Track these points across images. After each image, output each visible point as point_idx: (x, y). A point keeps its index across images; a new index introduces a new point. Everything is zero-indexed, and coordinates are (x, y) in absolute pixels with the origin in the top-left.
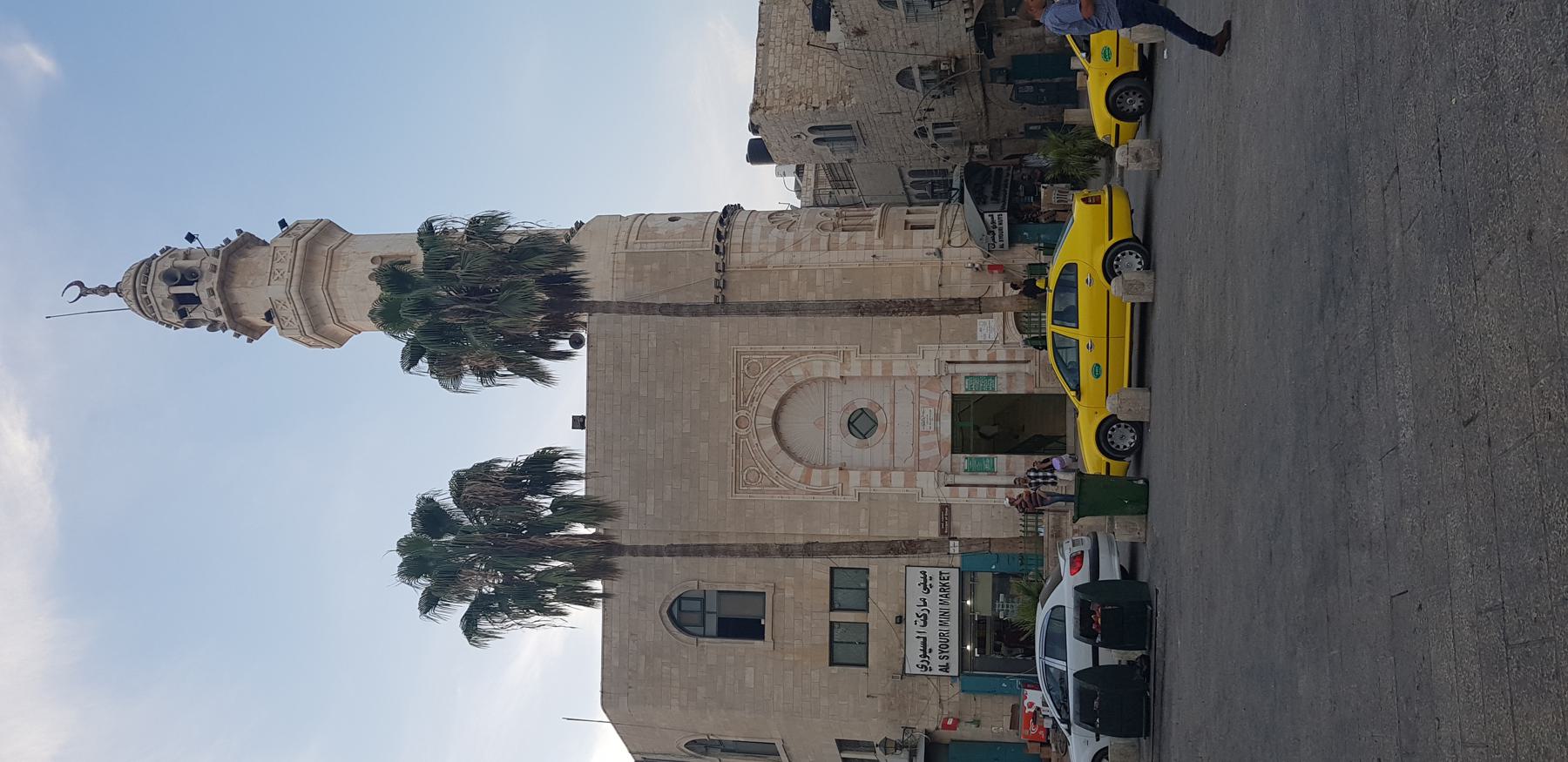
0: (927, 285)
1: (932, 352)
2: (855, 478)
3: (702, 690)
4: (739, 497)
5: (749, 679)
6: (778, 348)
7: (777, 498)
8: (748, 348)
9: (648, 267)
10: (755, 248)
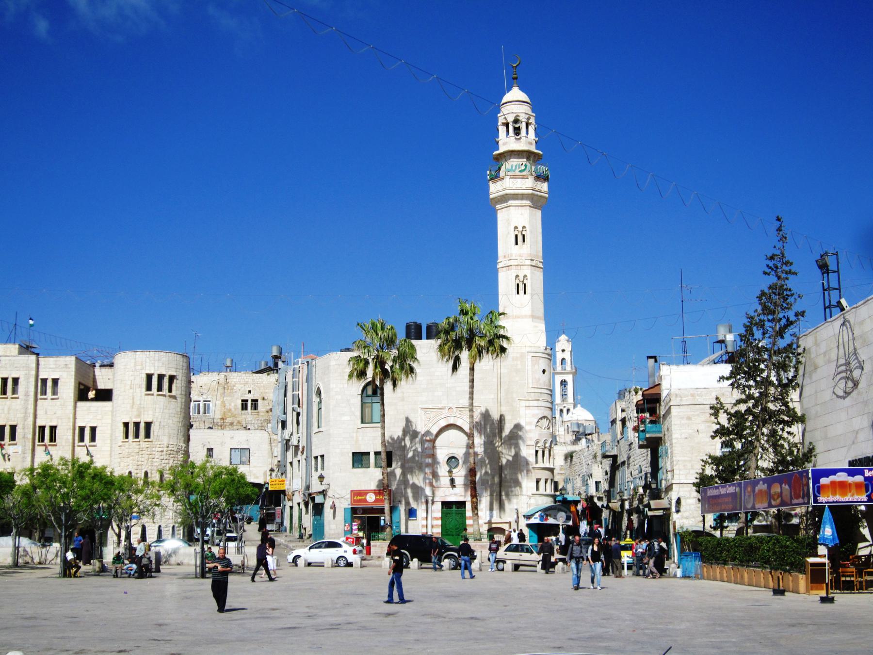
3: (340, 397)
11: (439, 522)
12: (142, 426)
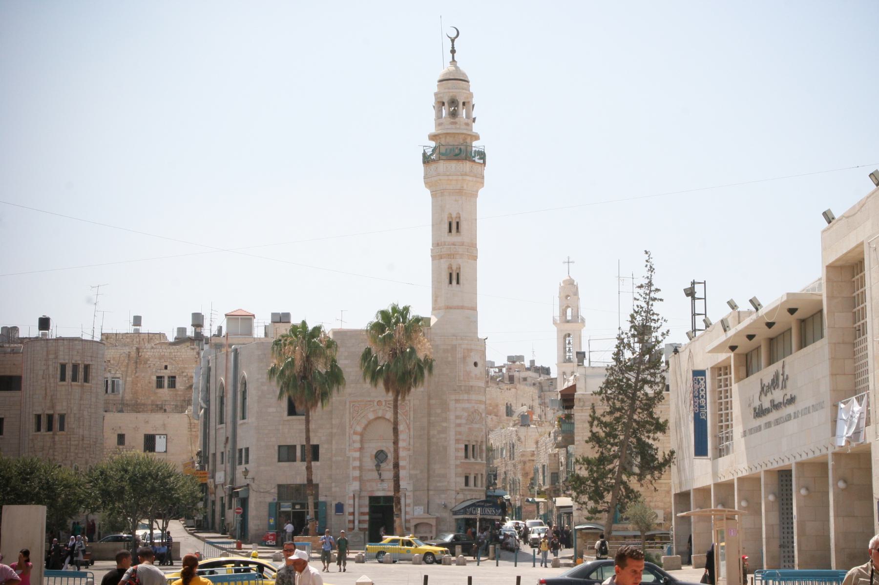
0: (439, 484)
1: (410, 488)
2: (357, 454)
3: (265, 388)
4: (348, 404)
5: (271, 410)
6: (412, 418)
7: (348, 420)
10: (458, 405)
11: (367, 518)
12: (56, 417)
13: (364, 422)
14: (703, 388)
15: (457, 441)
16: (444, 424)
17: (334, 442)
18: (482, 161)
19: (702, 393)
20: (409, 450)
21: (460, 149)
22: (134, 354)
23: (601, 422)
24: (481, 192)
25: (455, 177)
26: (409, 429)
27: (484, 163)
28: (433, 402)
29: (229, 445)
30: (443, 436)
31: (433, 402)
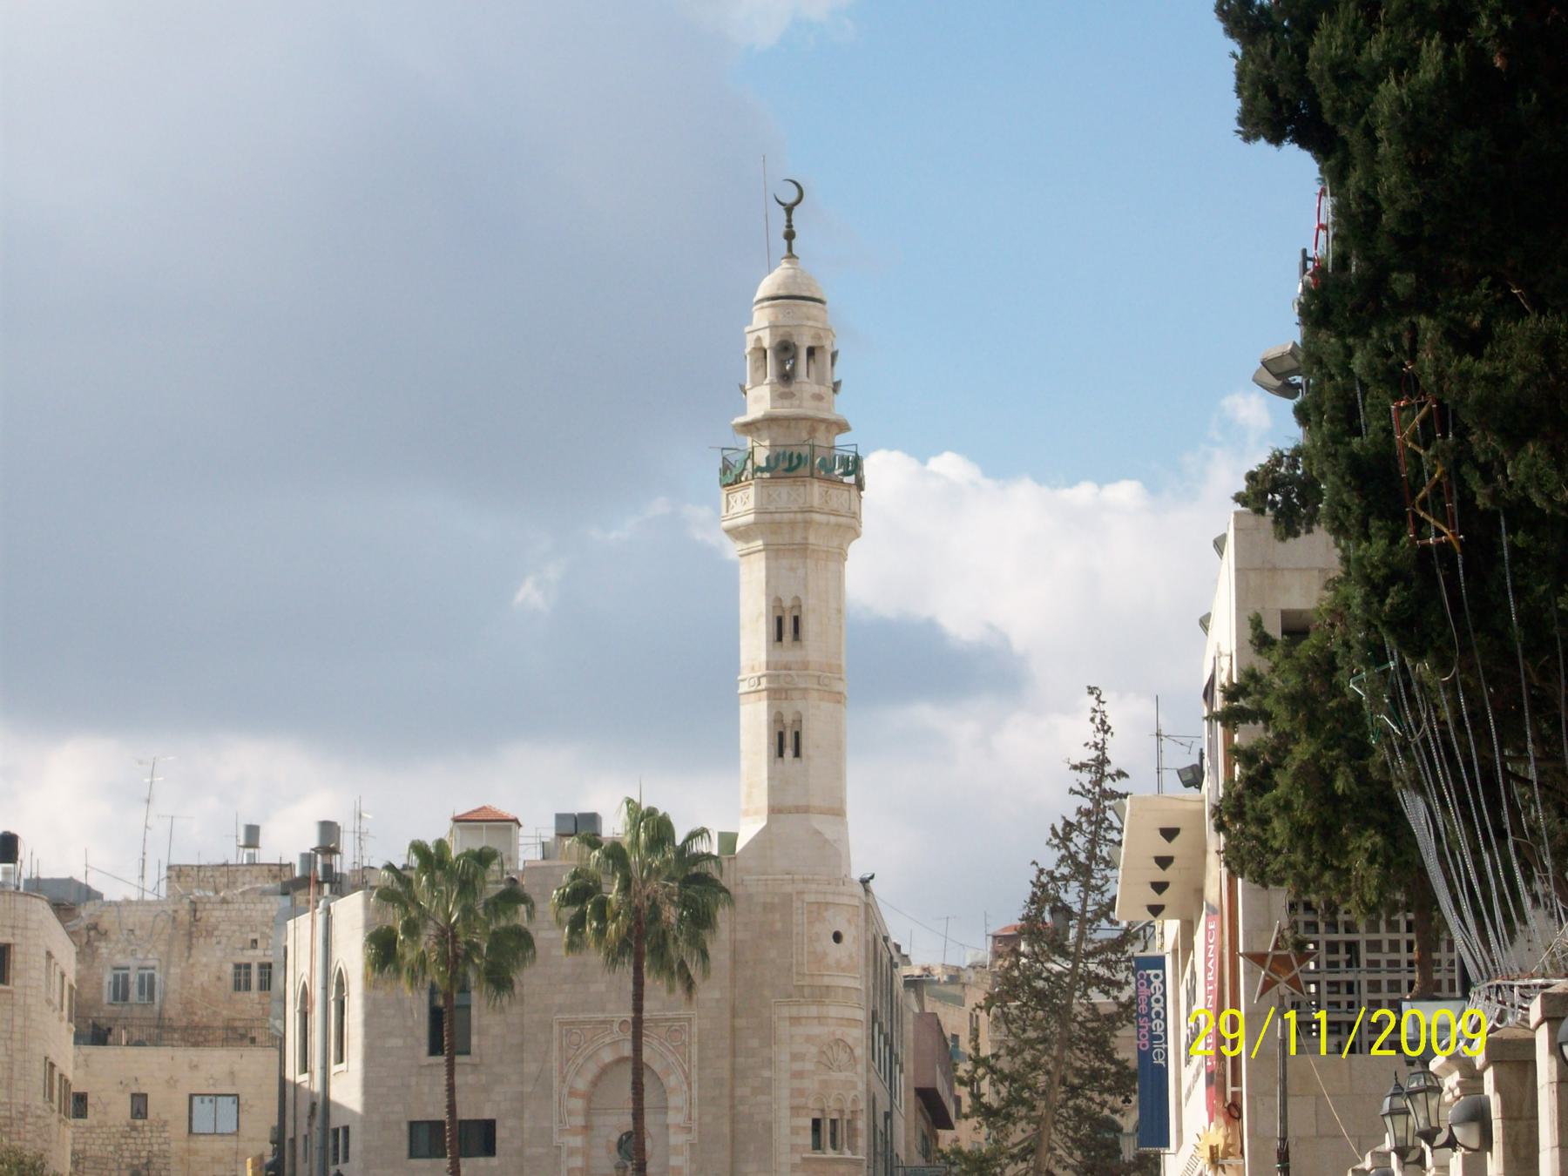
2: (577, 1141)
4: (556, 1028)
6: (695, 1058)
7: (556, 1065)
8: (695, 1029)
9: (777, 916)
13: (592, 1070)
14: (1158, 995)
15: (795, 1110)
16: (766, 1074)
17: (526, 1115)
18: (851, 479)
19: (1157, 1007)
20: (689, 1130)
21: (799, 456)
22: (184, 916)
23: (992, 1070)
24: (855, 550)
25: (786, 517)
26: (689, 1085)
27: (860, 485)
28: (741, 1022)
29: (317, 1122)
30: (762, 1098)
31: (741, 1022)
